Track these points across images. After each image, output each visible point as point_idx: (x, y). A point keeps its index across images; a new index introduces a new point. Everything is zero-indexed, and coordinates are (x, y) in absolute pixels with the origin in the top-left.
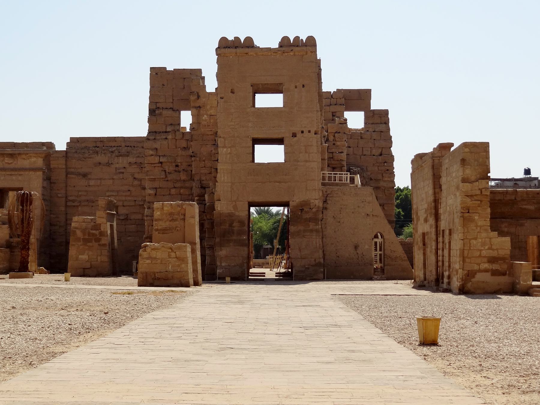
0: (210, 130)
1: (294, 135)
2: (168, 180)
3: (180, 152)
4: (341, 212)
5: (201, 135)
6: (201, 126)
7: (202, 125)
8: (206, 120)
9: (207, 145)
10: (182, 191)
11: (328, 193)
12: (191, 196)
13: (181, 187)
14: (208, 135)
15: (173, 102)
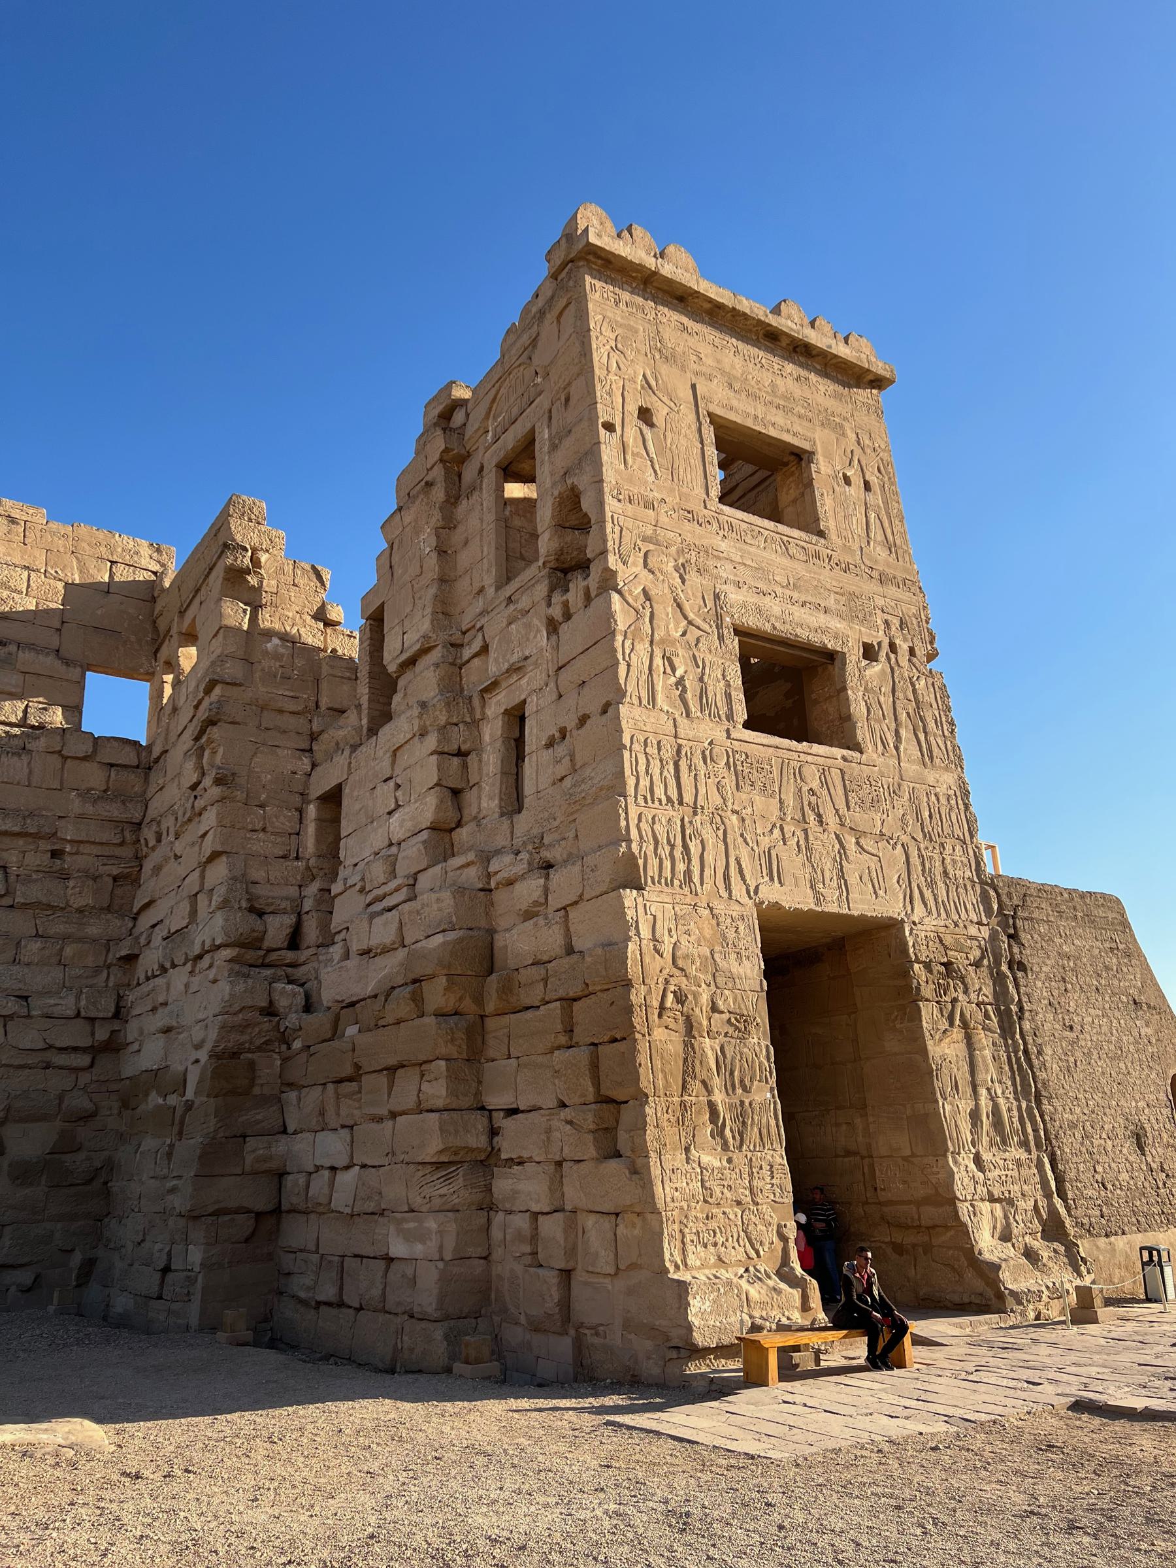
0: (291, 694)
1: (869, 652)
2: (12, 906)
3: (76, 805)
4: (1069, 986)
5: (254, 707)
6: (257, 675)
7: (263, 670)
8: (277, 656)
9: (278, 750)
10: (69, 951)
11: (1016, 901)
12: (105, 972)
13: (65, 938)
14: (281, 712)
15: (59, 630)
